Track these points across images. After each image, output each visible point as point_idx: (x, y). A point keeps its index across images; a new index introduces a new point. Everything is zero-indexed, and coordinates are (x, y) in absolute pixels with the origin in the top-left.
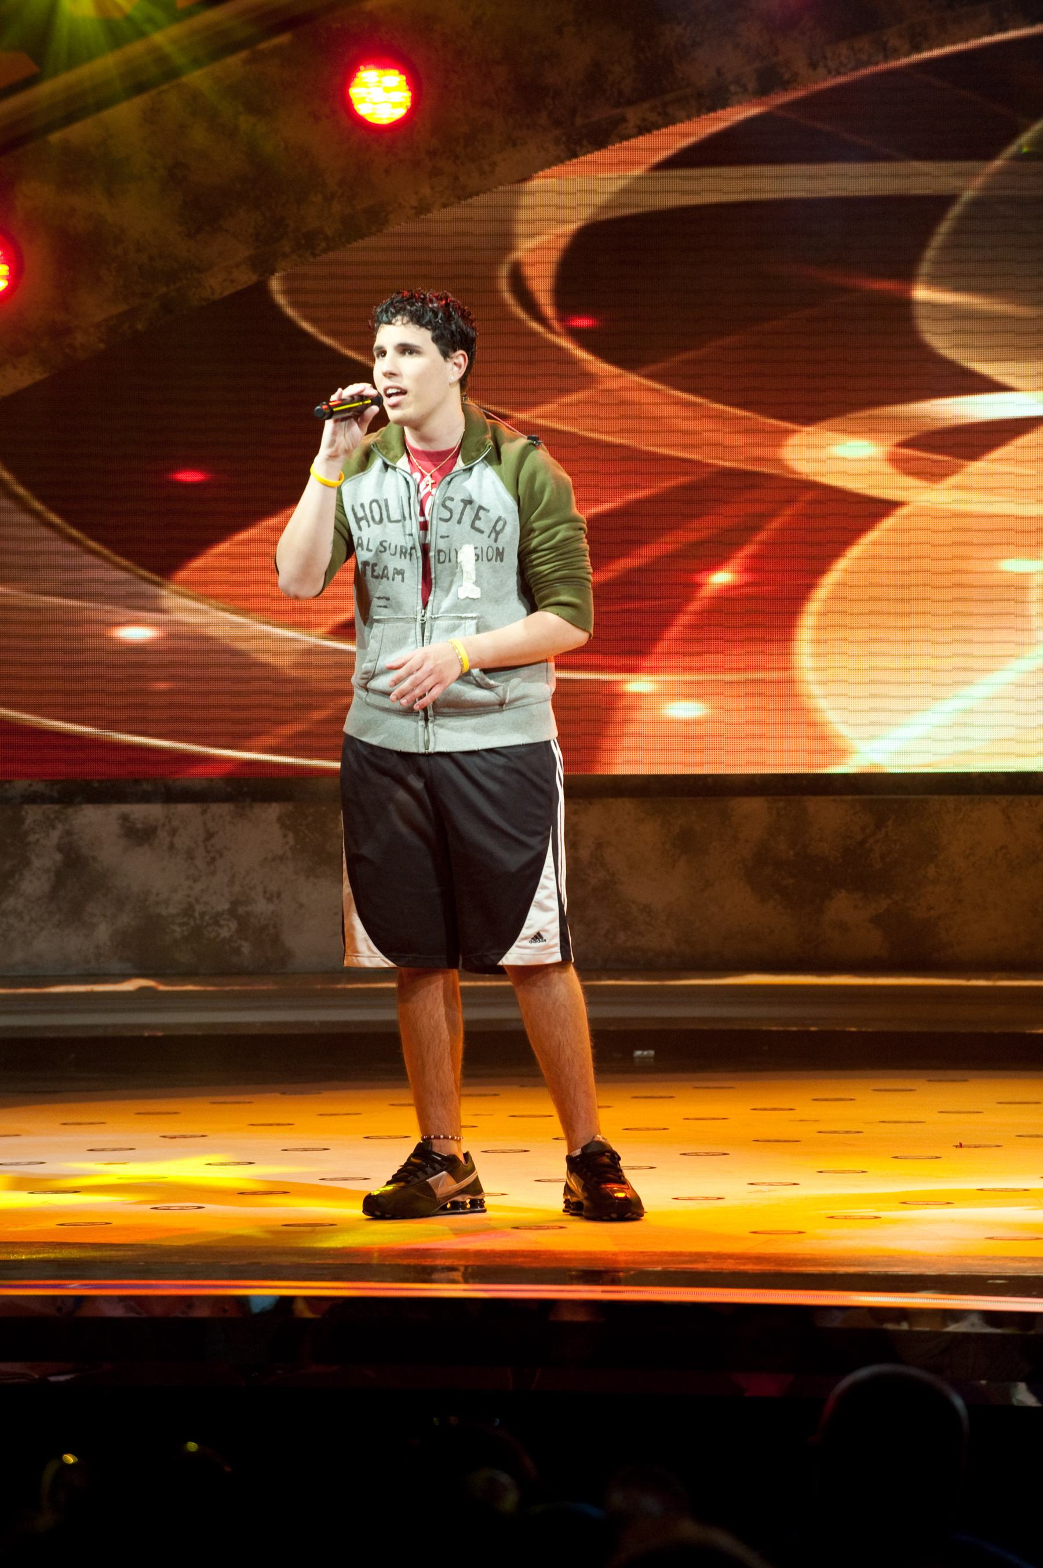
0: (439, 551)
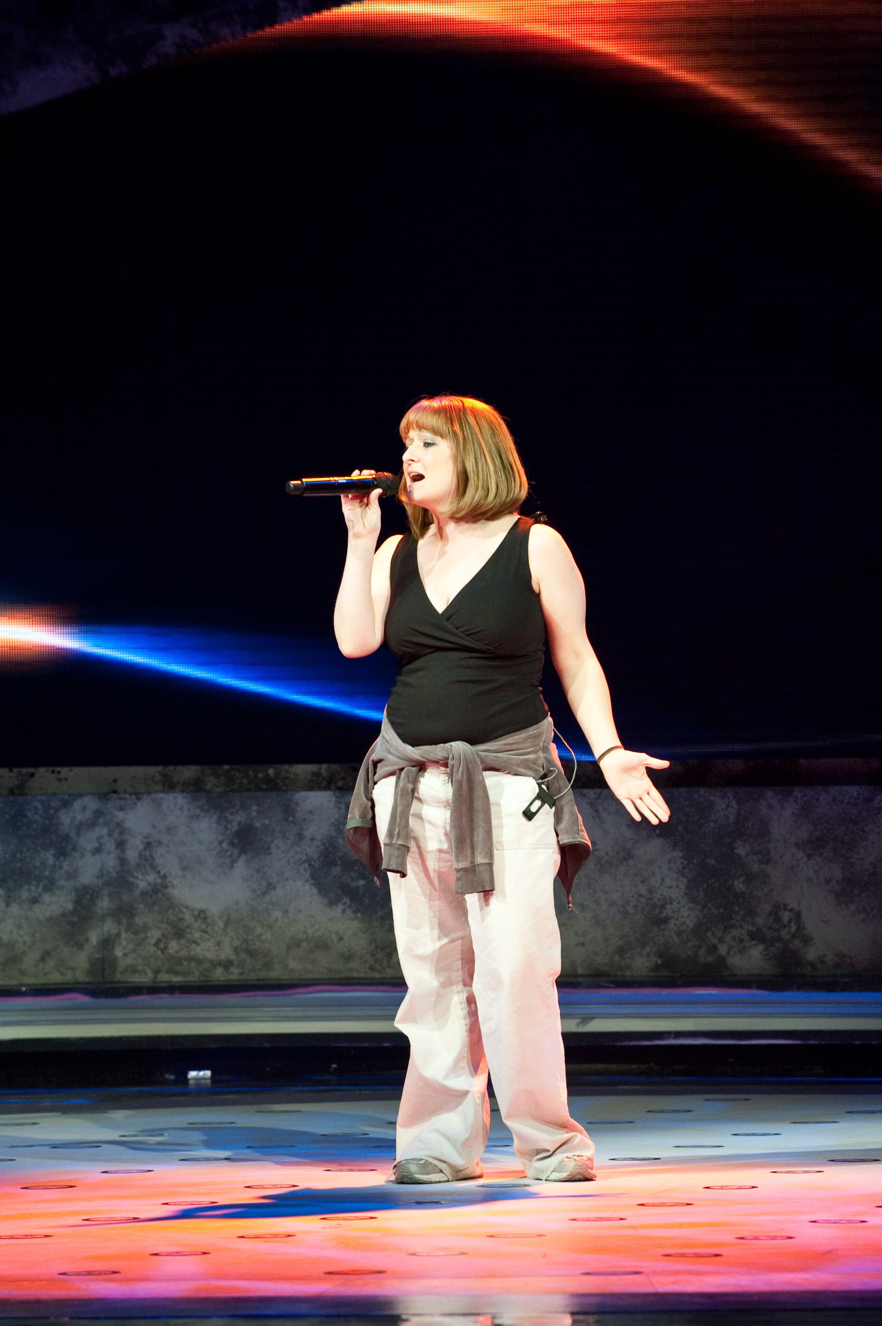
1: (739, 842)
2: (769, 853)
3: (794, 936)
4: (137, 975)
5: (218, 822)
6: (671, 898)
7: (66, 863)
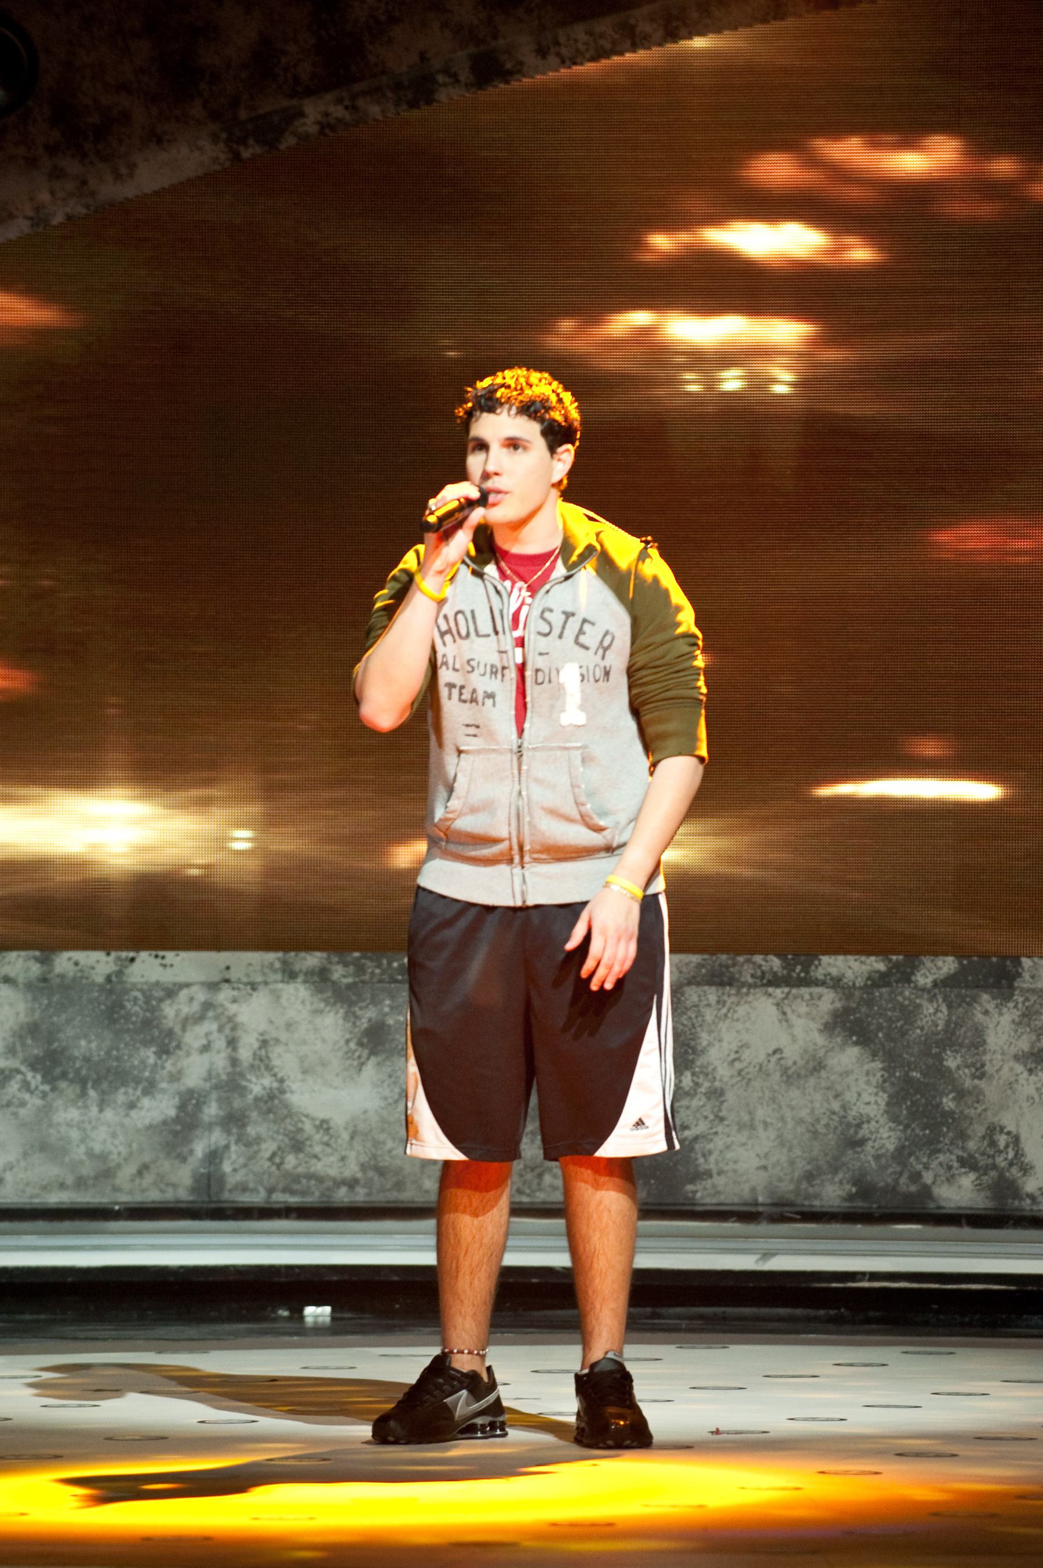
0: (537, 671)
1: (948, 1052)
2: (983, 1065)
3: (1011, 1164)
4: (247, 1194)
5: (345, 1018)
7: (170, 1062)
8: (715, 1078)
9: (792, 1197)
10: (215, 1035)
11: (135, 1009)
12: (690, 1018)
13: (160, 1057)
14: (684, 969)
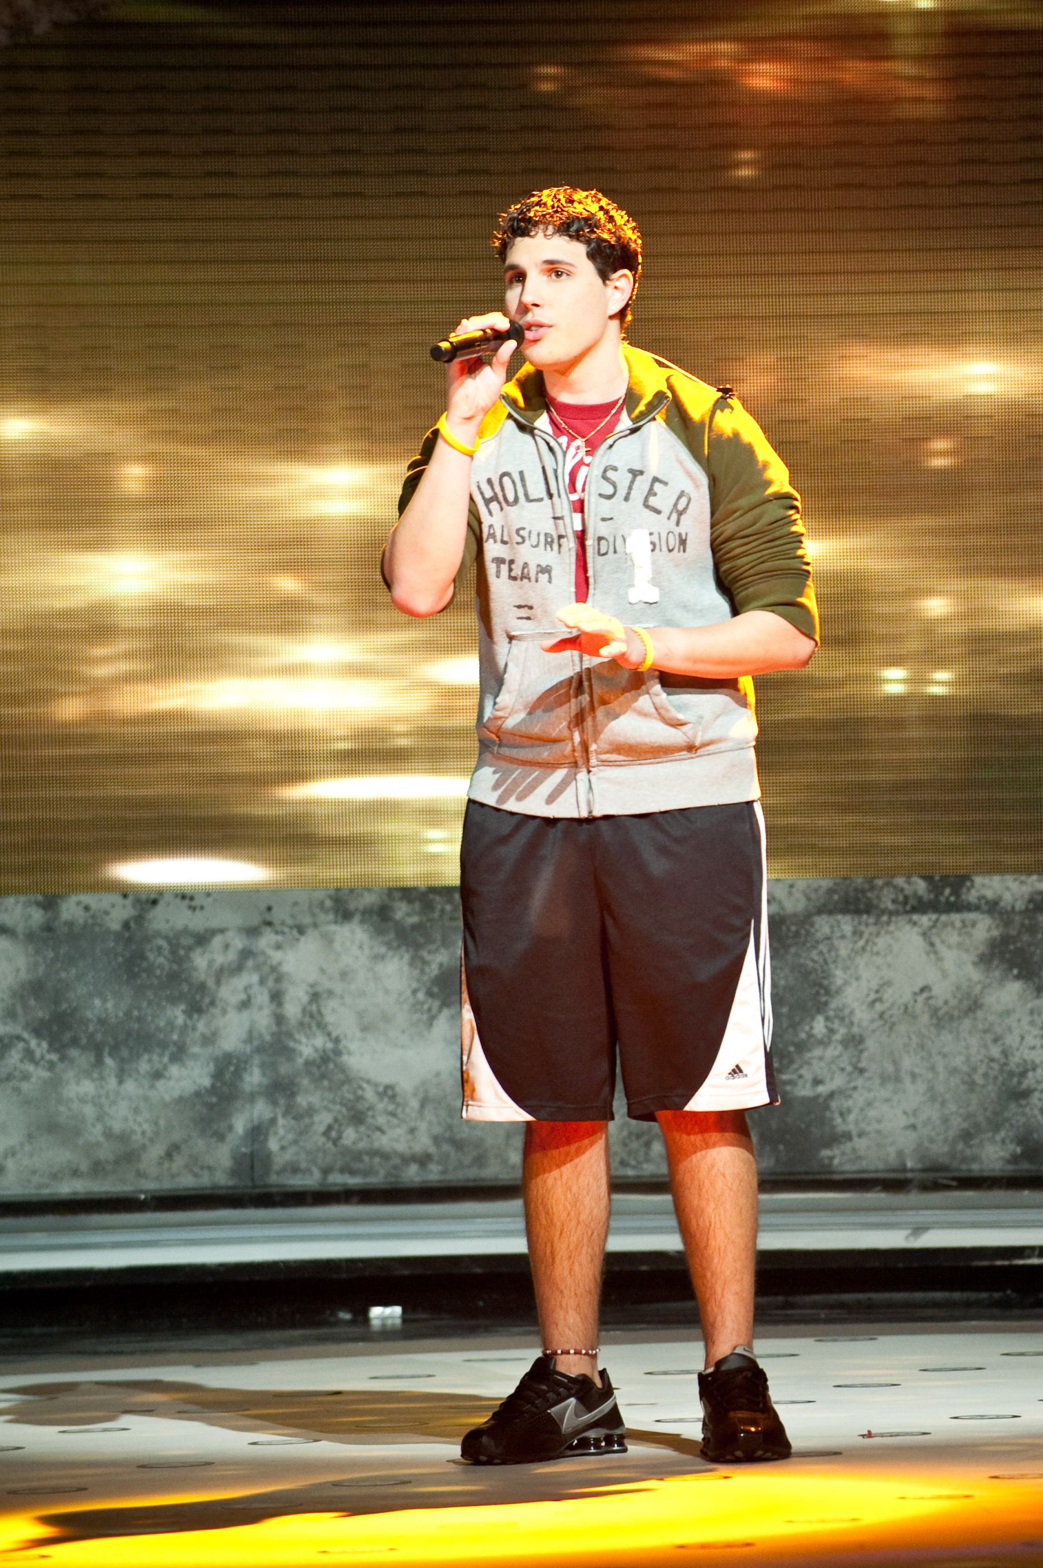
0: (600, 539)
4: (299, 1176)
5: (412, 964)
6: (1033, 1062)
8: (852, 1024)
9: (945, 1160)
10: (256, 989)
11: (160, 961)
12: (821, 953)
13: (190, 1017)
14: (813, 896)
